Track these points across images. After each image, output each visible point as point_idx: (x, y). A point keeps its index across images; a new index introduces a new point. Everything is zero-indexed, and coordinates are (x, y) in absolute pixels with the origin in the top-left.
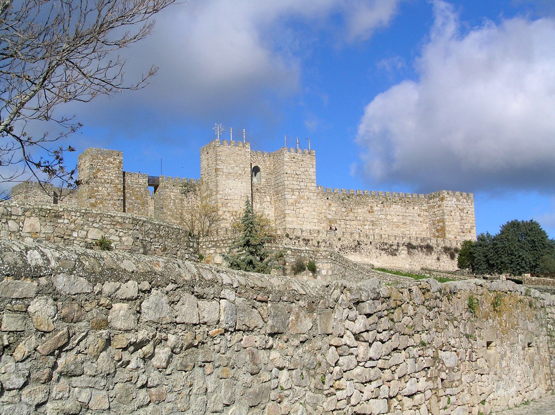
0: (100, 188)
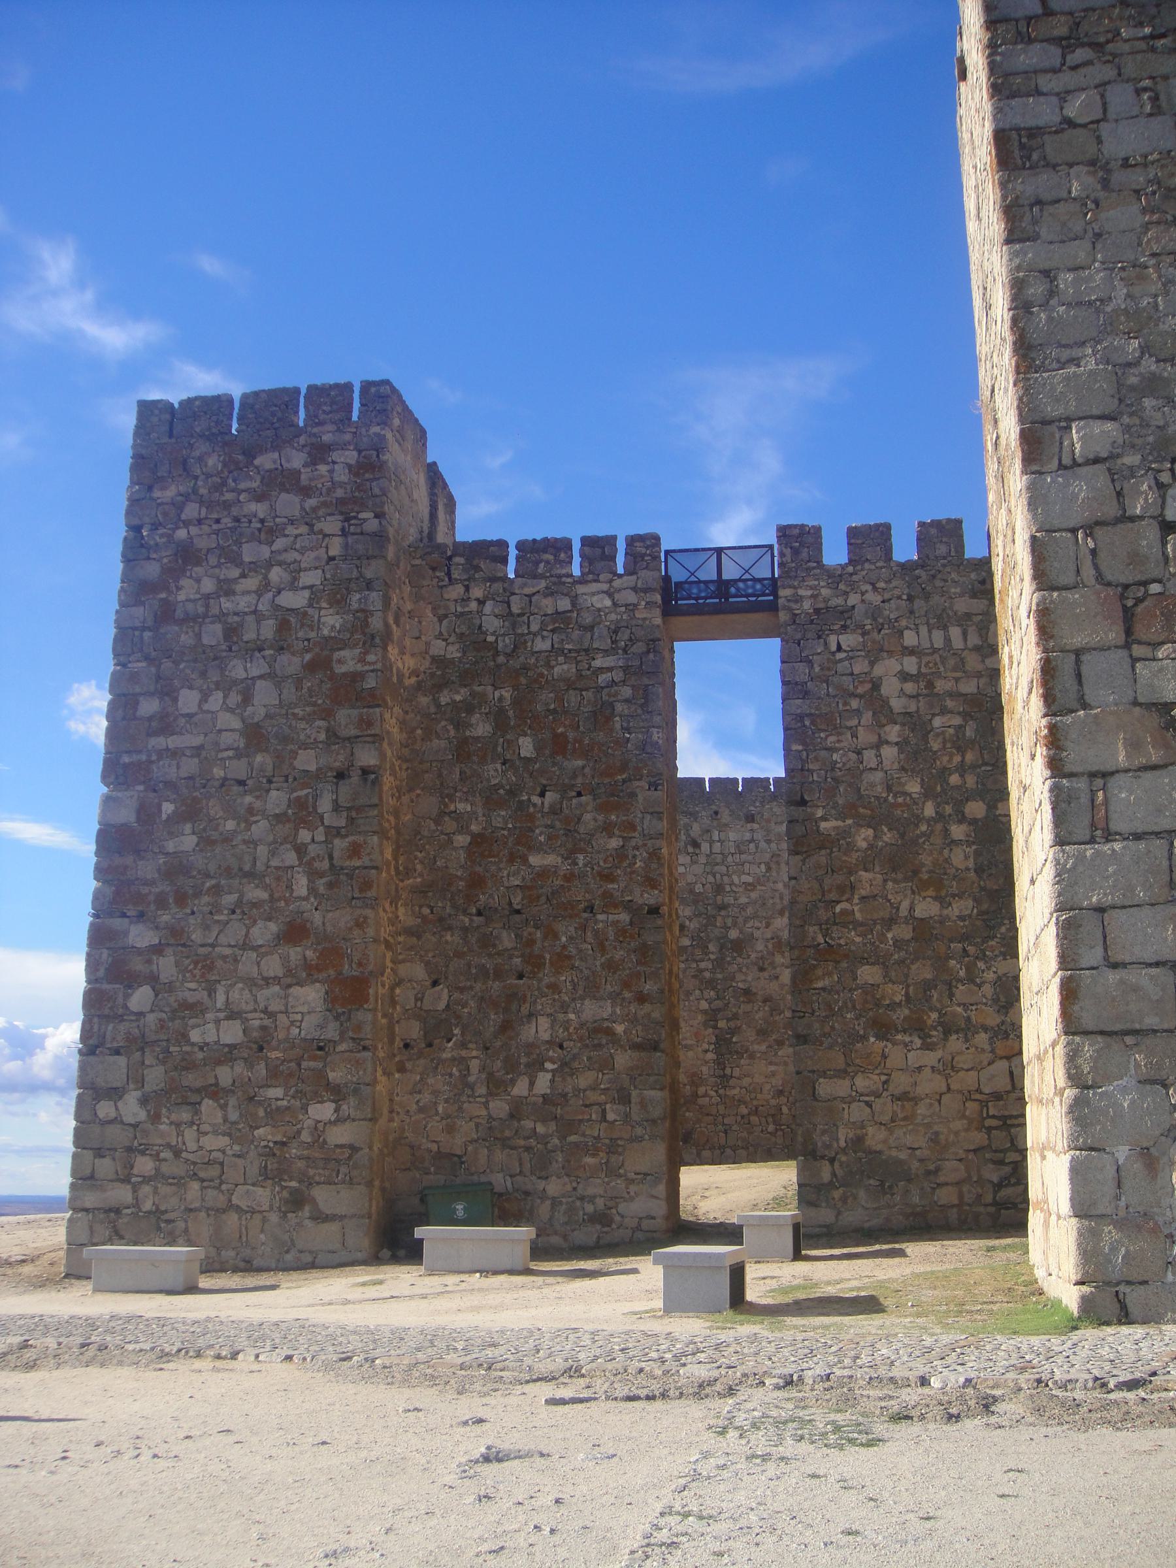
0: (188, 700)
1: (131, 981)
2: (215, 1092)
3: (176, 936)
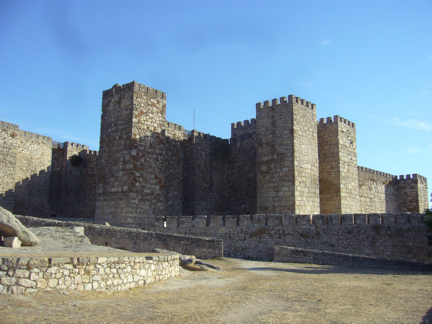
1: (136, 181)
2: (147, 200)
3: (142, 175)
